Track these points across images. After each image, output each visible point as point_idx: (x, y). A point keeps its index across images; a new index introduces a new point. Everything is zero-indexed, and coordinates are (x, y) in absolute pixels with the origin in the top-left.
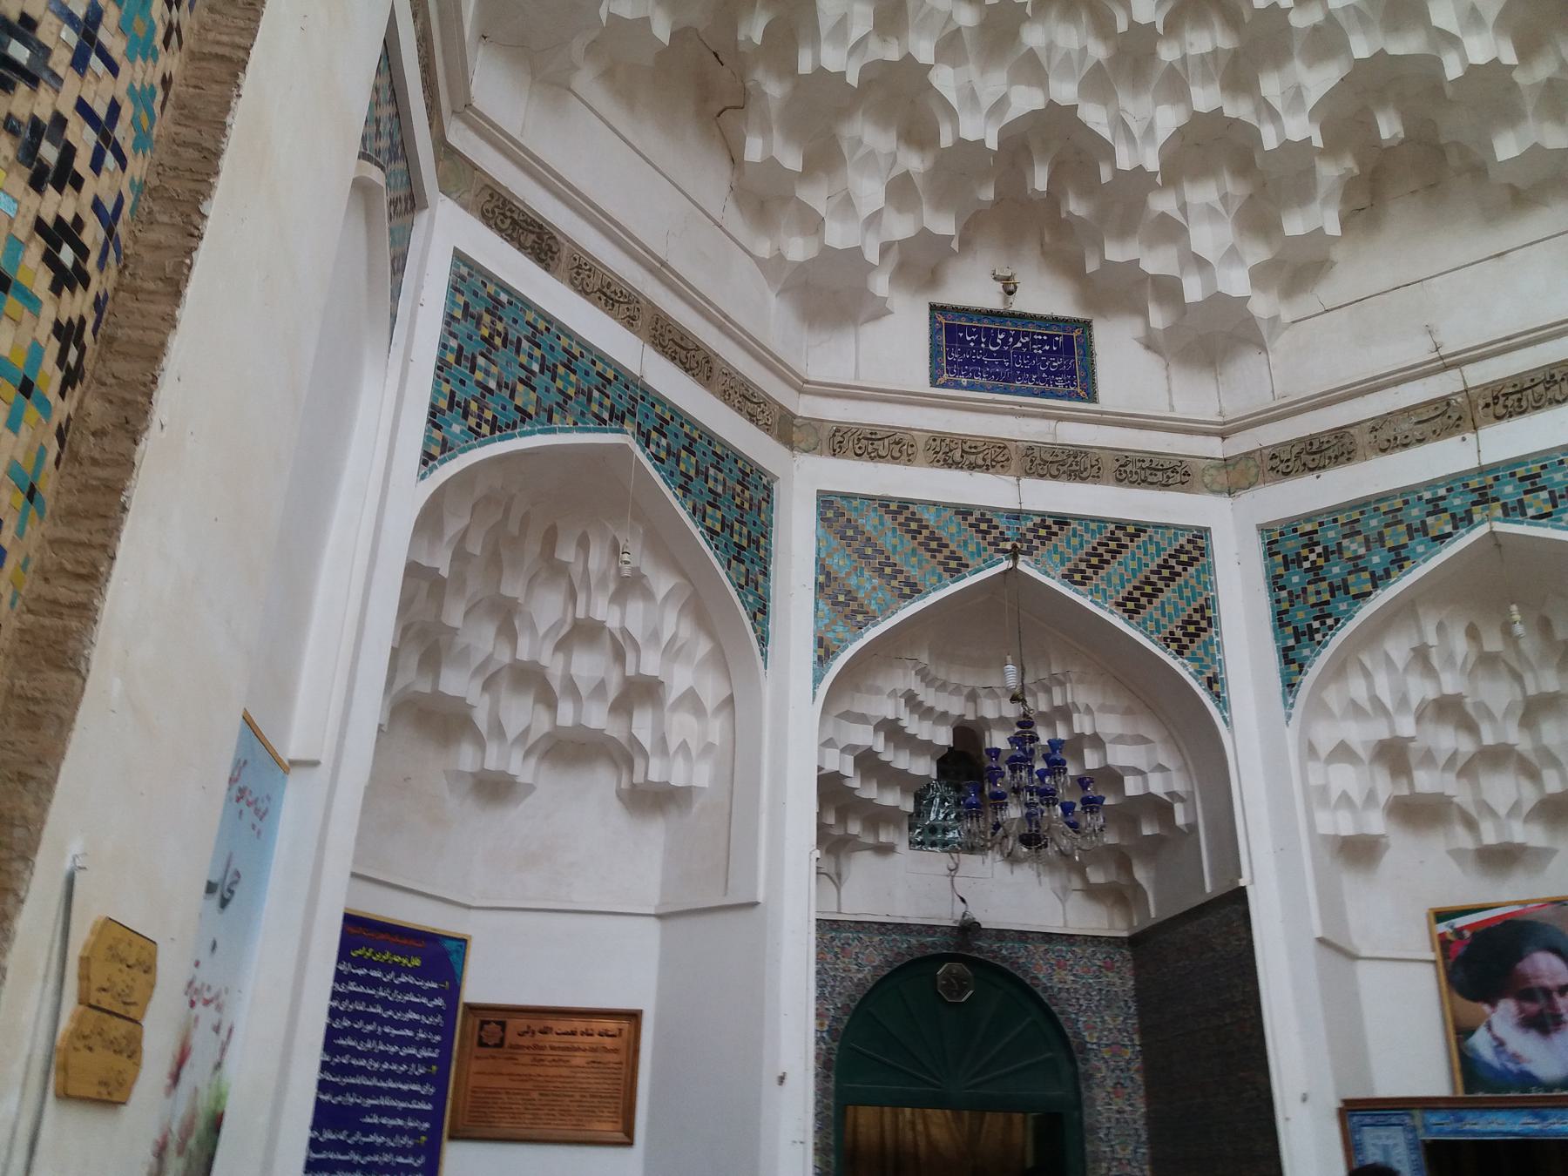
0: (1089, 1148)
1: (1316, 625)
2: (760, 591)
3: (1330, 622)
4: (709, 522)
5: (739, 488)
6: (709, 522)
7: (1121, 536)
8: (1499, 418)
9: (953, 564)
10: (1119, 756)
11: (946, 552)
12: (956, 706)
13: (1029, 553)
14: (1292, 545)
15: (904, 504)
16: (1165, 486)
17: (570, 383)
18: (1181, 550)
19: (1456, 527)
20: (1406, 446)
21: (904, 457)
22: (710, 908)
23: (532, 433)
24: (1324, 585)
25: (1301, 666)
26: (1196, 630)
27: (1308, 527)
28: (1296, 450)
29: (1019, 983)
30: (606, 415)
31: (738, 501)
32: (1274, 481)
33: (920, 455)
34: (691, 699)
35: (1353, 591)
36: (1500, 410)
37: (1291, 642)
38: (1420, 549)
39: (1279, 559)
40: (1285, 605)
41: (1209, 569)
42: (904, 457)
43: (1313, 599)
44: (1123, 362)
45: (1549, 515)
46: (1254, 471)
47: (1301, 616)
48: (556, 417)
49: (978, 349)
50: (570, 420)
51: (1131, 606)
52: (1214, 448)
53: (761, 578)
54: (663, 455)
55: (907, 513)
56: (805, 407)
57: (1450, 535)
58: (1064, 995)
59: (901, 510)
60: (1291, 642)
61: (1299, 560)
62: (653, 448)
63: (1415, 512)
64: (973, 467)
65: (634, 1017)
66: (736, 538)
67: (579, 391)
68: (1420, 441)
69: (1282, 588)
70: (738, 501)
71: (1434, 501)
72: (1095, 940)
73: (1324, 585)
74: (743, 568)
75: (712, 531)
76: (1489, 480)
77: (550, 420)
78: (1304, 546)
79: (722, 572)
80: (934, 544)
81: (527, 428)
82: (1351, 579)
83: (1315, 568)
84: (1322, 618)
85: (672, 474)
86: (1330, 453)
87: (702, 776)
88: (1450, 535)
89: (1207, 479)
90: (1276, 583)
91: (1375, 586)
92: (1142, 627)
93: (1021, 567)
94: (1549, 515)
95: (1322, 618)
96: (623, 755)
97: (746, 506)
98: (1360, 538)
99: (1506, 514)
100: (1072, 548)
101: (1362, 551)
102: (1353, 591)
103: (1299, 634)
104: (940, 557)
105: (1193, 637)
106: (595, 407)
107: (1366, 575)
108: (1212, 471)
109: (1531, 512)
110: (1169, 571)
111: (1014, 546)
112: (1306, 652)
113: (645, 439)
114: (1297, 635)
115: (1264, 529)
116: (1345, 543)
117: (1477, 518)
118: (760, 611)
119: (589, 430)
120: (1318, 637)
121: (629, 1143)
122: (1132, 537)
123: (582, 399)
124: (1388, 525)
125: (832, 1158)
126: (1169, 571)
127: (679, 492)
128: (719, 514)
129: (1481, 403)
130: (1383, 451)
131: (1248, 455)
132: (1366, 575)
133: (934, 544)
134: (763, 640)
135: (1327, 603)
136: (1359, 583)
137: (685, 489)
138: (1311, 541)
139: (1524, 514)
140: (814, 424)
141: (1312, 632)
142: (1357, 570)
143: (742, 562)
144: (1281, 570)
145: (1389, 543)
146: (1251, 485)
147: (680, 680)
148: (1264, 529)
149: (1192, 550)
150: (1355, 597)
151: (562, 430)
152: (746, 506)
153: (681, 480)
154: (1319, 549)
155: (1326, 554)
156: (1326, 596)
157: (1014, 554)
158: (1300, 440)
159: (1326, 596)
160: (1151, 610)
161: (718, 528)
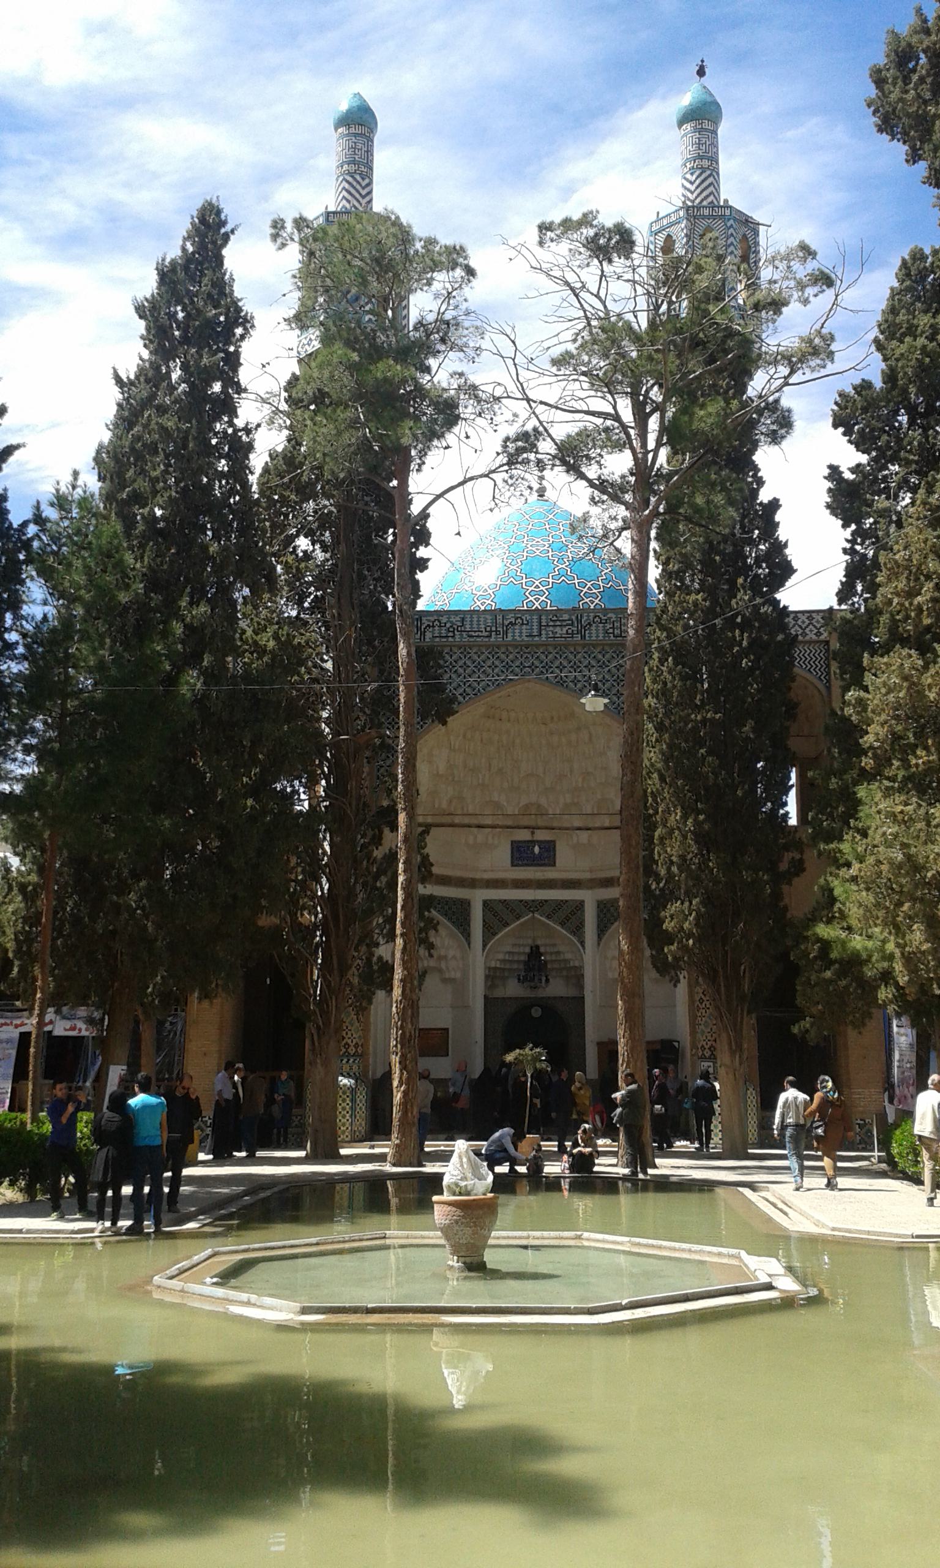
7: (560, 904)
10: (568, 956)
12: (530, 942)
22: (461, 1006)
26: (578, 930)
34: (454, 957)
44: (564, 854)
49: (521, 854)
51: (562, 924)
56: (478, 876)
59: (504, 902)
65: (447, 1030)
80: (512, 911)
87: (458, 975)
90: (598, 916)
96: (440, 971)
110: (573, 913)
118: (467, 936)
133: (512, 911)
134: (469, 944)
138: (602, 911)
140: (481, 880)
147: (451, 953)
149: (582, 903)
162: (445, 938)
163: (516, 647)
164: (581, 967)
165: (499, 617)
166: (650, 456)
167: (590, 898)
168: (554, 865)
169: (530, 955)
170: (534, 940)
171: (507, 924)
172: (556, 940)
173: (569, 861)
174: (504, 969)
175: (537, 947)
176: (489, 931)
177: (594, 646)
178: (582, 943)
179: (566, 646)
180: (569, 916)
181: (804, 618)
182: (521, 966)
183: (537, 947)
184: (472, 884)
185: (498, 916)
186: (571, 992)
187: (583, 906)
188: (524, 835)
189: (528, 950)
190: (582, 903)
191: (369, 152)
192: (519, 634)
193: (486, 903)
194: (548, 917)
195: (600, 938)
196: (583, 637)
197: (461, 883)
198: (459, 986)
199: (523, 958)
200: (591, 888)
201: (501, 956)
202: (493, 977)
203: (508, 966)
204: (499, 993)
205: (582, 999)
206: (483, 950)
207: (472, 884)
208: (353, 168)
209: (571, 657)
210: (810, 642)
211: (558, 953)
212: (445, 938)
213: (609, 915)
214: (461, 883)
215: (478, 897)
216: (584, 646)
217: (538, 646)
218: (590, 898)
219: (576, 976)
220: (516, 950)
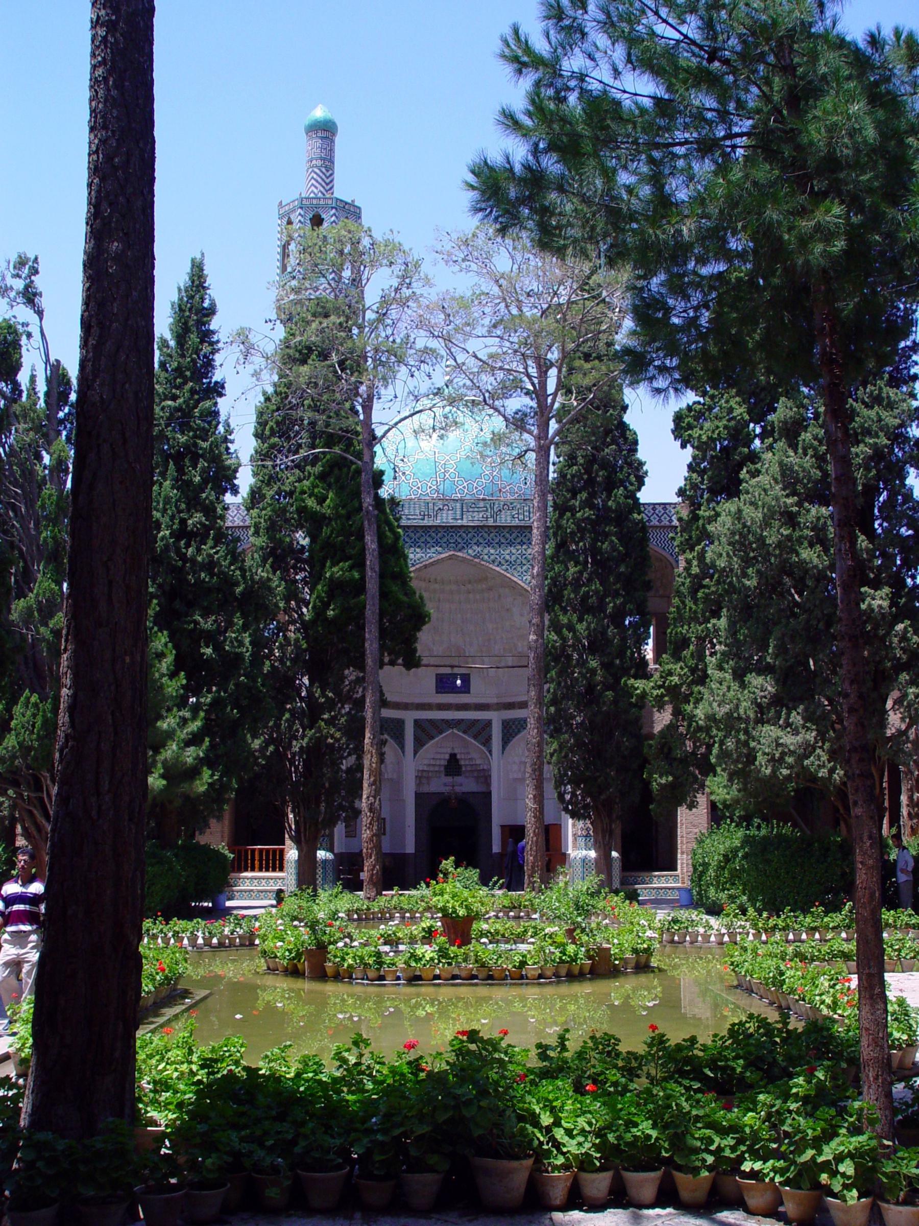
12: (449, 751)
26: (487, 742)
49: (444, 684)
51: (475, 737)
52: (495, 701)
103: (506, 741)
110: (483, 729)
118: (402, 747)
126: (483, 729)
149: (489, 723)
162: (390, 749)
163: (443, 527)
164: (489, 770)
165: (431, 505)
166: (549, 400)
167: (496, 718)
168: (468, 692)
169: (449, 761)
171: (433, 738)
172: (470, 751)
173: (480, 692)
174: (428, 771)
175: (455, 755)
176: (419, 743)
177: (504, 527)
178: (490, 752)
179: (482, 527)
180: (481, 731)
181: (660, 508)
182: (442, 769)
183: (455, 755)
184: (406, 706)
185: (426, 732)
186: (482, 789)
188: (448, 671)
189: (447, 757)
190: (489, 723)
191: (332, 150)
192: (446, 518)
193: (416, 722)
194: (464, 732)
195: (504, 748)
196: (495, 521)
197: (397, 706)
198: (397, 785)
201: (426, 762)
202: (421, 777)
203: (432, 769)
204: (425, 789)
205: (489, 794)
207: (406, 706)
208: (319, 163)
209: (486, 535)
210: (664, 527)
211: (471, 759)
212: (390, 749)
214: (397, 706)
215: (409, 718)
216: (496, 527)
217: (462, 526)
218: (496, 718)
219: (485, 777)
220: (439, 756)
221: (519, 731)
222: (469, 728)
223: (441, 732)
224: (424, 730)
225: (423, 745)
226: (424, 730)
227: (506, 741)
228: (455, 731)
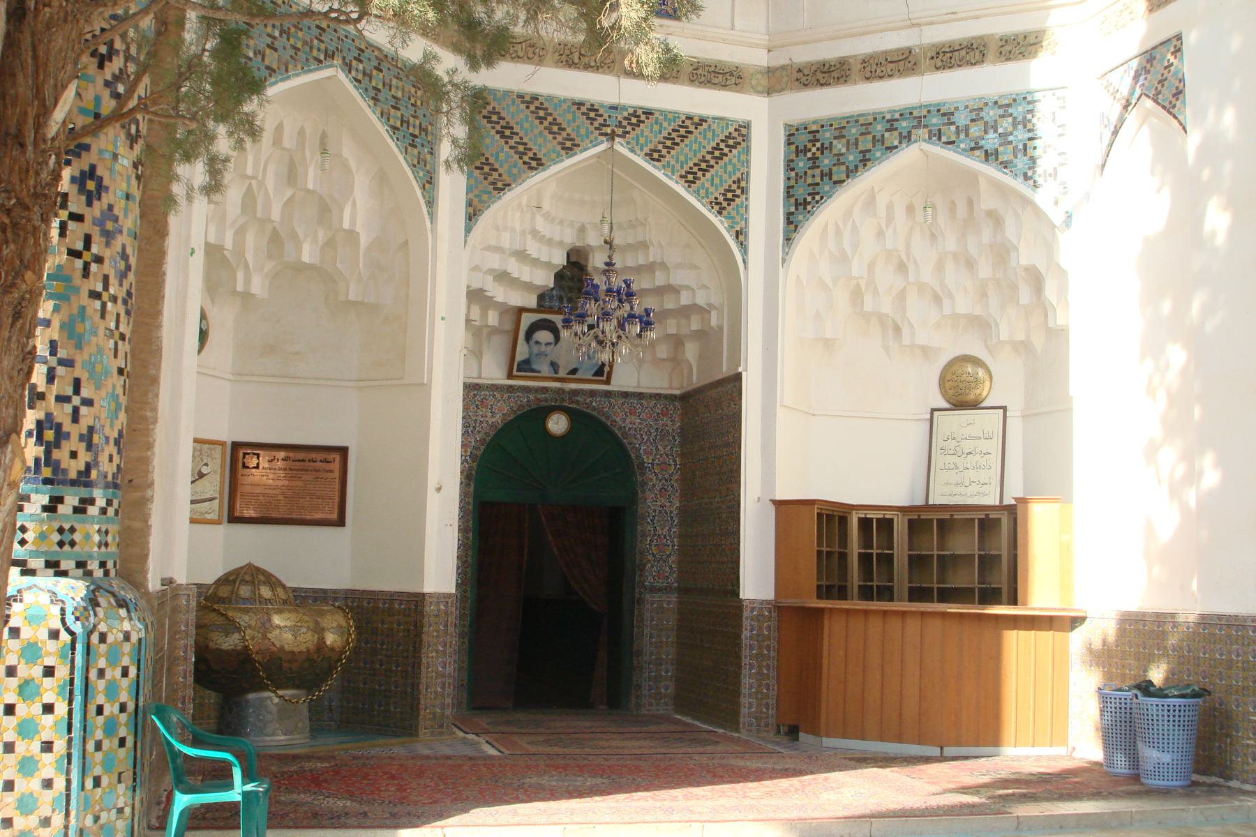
0: (639, 528)
1: (809, 199)
2: (428, 167)
3: (817, 198)
4: (392, 122)
5: (413, 90)
6: (392, 122)
7: (688, 125)
8: (937, 69)
9: (568, 144)
10: (677, 278)
11: (564, 134)
12: (570, 238)
13: (622, 136)
14: (802, 139)
15: (535, 98)
16: (724, 86)
17: (299, 39)
18: (729, 137)
19: (900, 142)
20: (881, 77)
21: (536, 58)
23: (276, 83)
24: (817, 172)
25: (796, 227)
26: (732, 197)
27: (814, 128)
28: (814, 68)
29: (604, 426)
30: (322, 57)
31: (413, 101)
32: (799, 89)
33: (549, 57)
35: (835, 178)
36: (939, 64)
37: (793, 209)
38: (878, 154)
39: (793, 148)
40: (792, 182)
41: (748, 151)
42: (536, 58)
43: (810, 180)
45: (953, 143)
46: (785, 79)
47: (801, 192)
48: (290, 67)
50: (299, 67)
51: (690, 178)
53: (428, 157)
54: (360, 77)
55: (537, 104)
57: (896, 147)
58: (632, 432)
59: (532, 102)
60: (793, 209)
61: (806, 150)
62: (354, 73)
63: (879, 127)
64: (587, 67)
65: (343, 451)
66: (411, 130)
67: (305, 43)
68: (890, 76)
69: (792, 170)
70: (413, 101)
71: (891, 121)
72: (658, 396)
73: (817, 172)
74: (415, 152)
75: (395, 128)
76: (924, 112)
77: (287, 71)
78: (810, 141)
79: (401, 158)
80: (555, 128)
81: (273, 80)
82: (835, 169)
83: (814, 158)
84: (812, 194)
85: (366, 90)
86: (835, 74)
88: (896, 147)
89: (754, 82)
90: (790, 165)
91: (848, 177)
92: (697, 193)
93: (617, 147)
94: (953, 143)
95: (812, 194)
97: (419, 103)
98: (844, 141)
99: (930, 138)
100: (650, 134)
101: (844, 150)
102: (835, 178)
103: (801, 203)
104: (559, 138)
105: (730, 201)
106: (315, 53)
107: (843, 168)
108: (759, 76)
109: (944, 139)
110: (718, 153)
111: (613, 131)
112: (801, 217)
113: (348, 67)
114: (797, 205)
115: (787, 126)
116: (835, 142)
117: (913, 138)
119: (311, 71)
120: (809, 207)
121: (341, 522)
122: (697, 125)
123: (307, 49)
124: (862, 134)
125: (470, 535)
126: (718, 153)
127: (371, 103)
128: (399, 114)
129: (929, 55)
130: (868, 79)
131: (783, 67)
132: (843, 168)
133: (555, 128)
135: (818, 184)
136: (839, 173)
137: (375, 99)
139: (940, 139)
141: (806, 203)
142: (839, 163)
143: (415, 147)
144: (793, 156)
145: (861, 148)
146: (782, 90)
148: (787, 126)
149: (737, 137)
150: (835, 183)
151: (297, 75)
152: (419, 103)
153: (372, 93)
154: (818, 145)
155: (822, 149)
156: (818, 180)
157: (611, 137)
158: (818, 62)
159: (818, 180)
160: (704, 181)
161: (398, 124)
170: (582, 230)
171: (536, 163)
178: (740, 235)
180: (711, 157)
187: (746, 138)
189: (560, 259)
190: (738, 137)
195: (792, 224)
199: (518, 299)
200: (769, 92)
206: (468, 230)
213: (826, 162)
218: (765, 119)
221: (865, 160)
222: (671, 143)
223: (570, 147)
224: (506, 132)
225: (500, 187)
226: (506, 132)
227: (801, 203)
228: (620, 147)
